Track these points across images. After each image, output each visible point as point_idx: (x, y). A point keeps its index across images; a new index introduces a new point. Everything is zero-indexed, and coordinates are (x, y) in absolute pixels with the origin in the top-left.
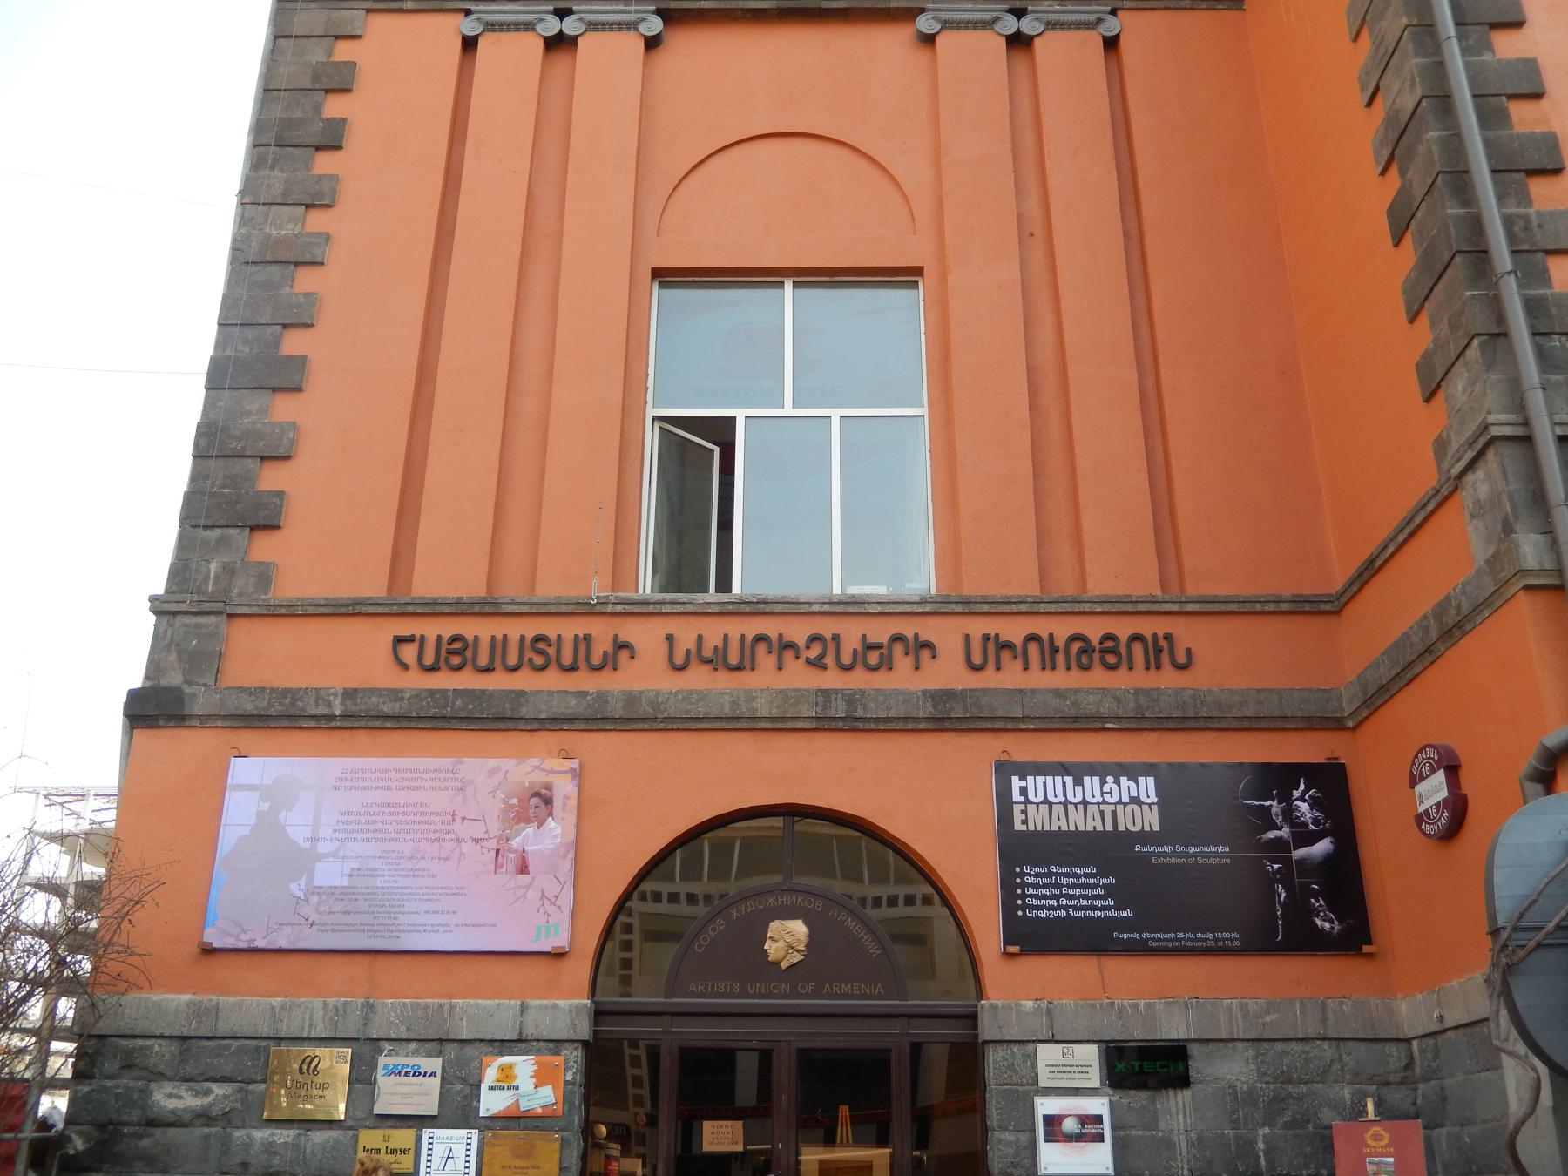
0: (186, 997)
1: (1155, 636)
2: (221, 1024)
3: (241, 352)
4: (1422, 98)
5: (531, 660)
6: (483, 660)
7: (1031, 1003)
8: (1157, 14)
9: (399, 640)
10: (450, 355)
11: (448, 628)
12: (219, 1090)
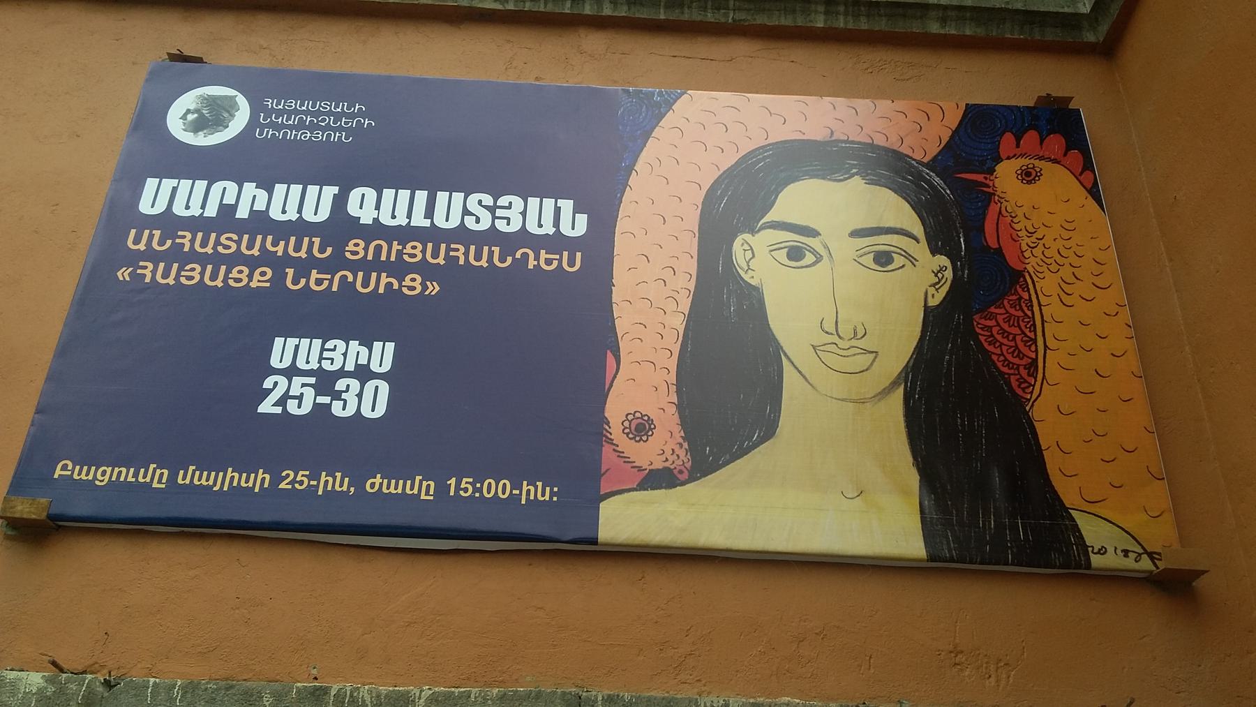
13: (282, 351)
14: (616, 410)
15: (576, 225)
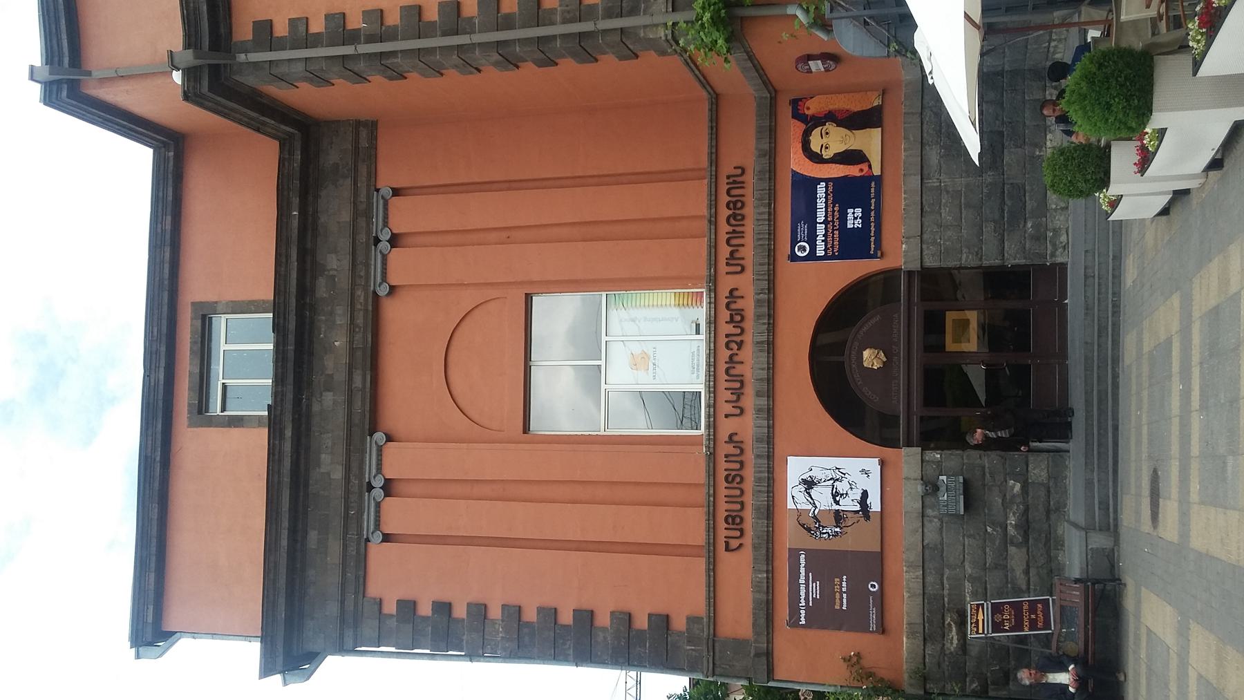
0: (905, 639)
1: (727, 184)
2: (918, 621)
3: (570, 645)
4: (498, 52)
5: (737, 483)
7: (904, 246)
8: (378, 168)
9: (727, 549)
11: (722, 525)
12: (948, 620)
13: (850, 226)
14: (859, 174)
15: (823, 184)
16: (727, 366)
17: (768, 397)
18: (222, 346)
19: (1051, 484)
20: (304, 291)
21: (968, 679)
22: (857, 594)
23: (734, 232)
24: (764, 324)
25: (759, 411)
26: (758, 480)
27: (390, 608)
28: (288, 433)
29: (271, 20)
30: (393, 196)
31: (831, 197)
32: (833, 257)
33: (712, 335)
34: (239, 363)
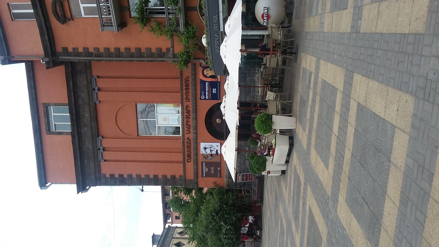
6: (190, 153)
9: (188, 162)
10: (152, 159)
11: (186, 157)
14: (215, 81)
15: (207, 83)
16: (186, 122)
17: (196, 130)
18: (53, 114)
19: (254, 148)
20: (76, 102)
21: (237, 185)
22: (215, 170)
23: (187, 92)
24: (195, 114)
25: (194, 133)
26: (194, 148)
27: (108, 176)
28: (77, 138)
29: (67, 47)
30: (97, 78)
31: (209, 86)
32: (210, 99)
33: (183, 116)
34: (57, 118)
